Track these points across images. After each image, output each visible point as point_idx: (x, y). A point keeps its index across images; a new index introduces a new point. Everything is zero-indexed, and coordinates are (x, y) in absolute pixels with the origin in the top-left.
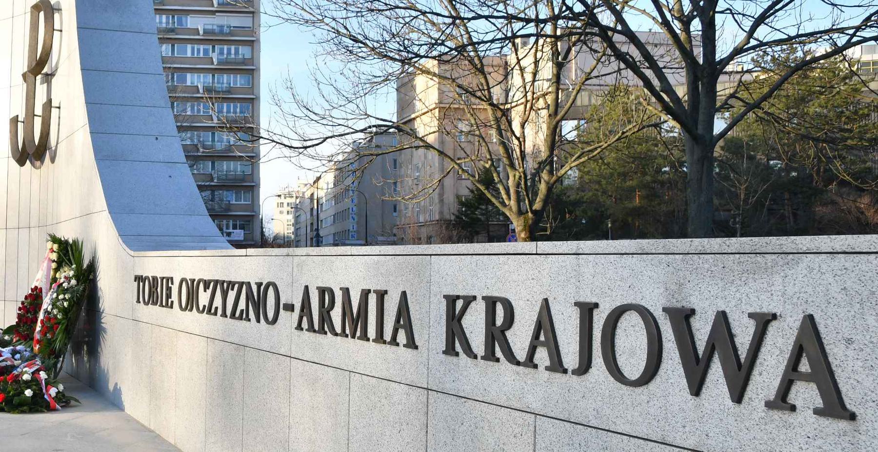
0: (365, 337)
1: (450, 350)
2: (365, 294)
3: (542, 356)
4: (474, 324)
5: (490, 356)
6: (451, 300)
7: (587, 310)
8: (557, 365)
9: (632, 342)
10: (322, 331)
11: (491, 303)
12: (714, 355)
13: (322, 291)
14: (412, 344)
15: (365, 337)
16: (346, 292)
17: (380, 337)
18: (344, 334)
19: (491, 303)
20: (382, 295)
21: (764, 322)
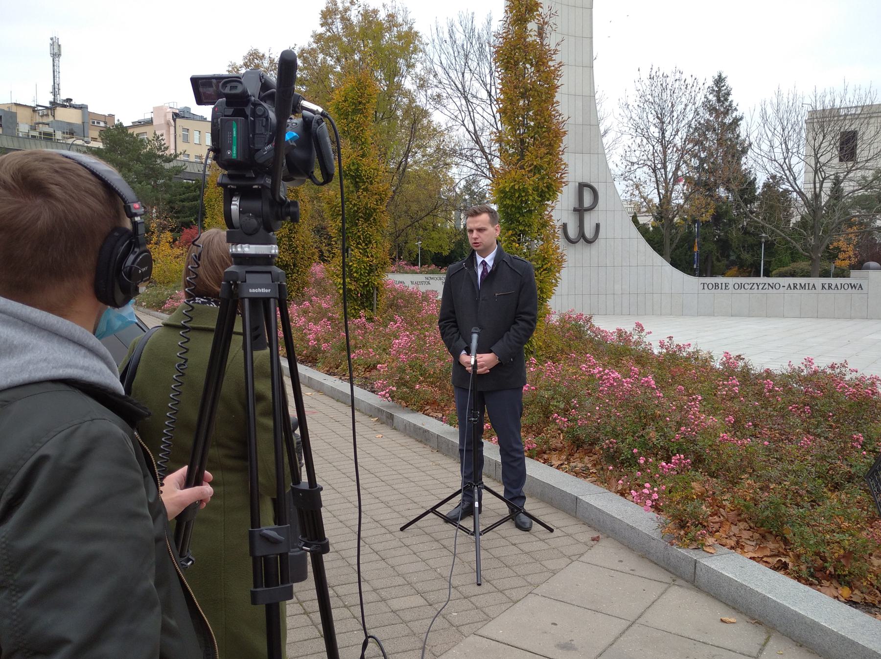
4: (826, 286)
9: (846, 287)
12: (853, 287)
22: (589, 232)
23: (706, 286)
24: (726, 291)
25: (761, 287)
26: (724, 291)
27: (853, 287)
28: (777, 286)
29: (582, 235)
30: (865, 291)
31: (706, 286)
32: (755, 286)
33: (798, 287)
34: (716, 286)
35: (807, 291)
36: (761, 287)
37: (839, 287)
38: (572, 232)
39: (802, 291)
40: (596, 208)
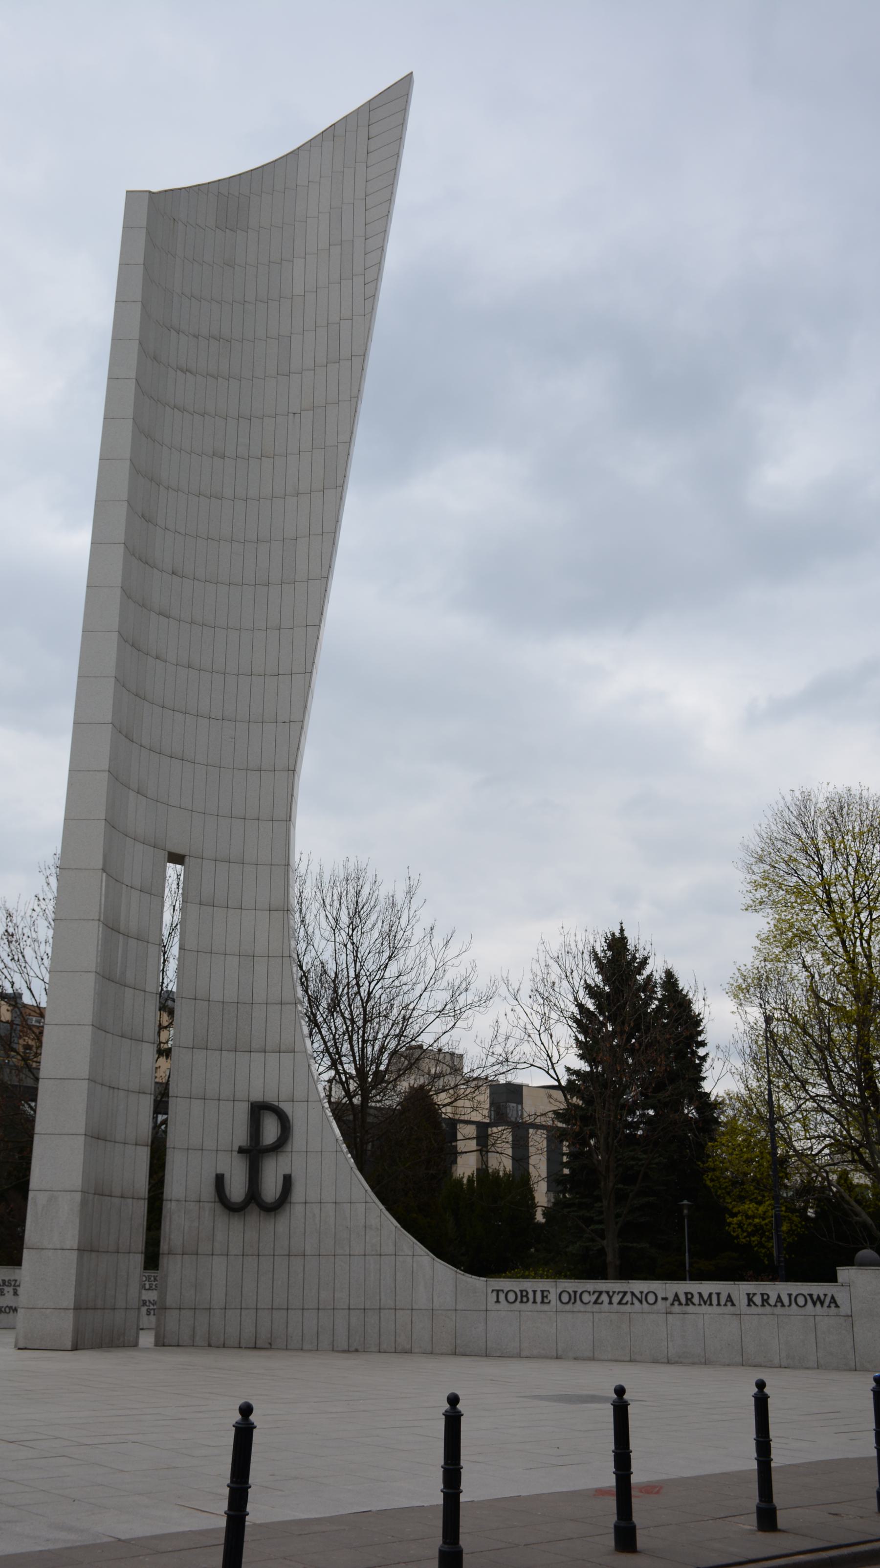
0: (711, 1304)
1: (749, 1305)
2: (710, 1295)
3: (779, 1304)
4: (758, 1300)
5: (763, 1305)
6: (748, 1295)
7: (790, 1295)
8: (783, 1305)
9: (801, 1301)
10: (687, 1304)
11: (762, 1295)
12: (818, 1301)
13: (686, 1294)
14: (733, 1305)
15: (711, 1304)
16: (700, 1294)
17: (719, 1304)
18: (700, 1305)
19: (762, 1295)
20: (718, 1294)
21: (825, 1295)
22: (271, 1189)
23: (502, 1296)
24: (545, 1307)
25: (616, 1299)
26: (538, 1306)
27: (818, 1301)
28: (651, 1298)
29: (253, 1195)
30: (844, 1309)
31: (502, 1296)
32: (605, 1298)
33: (696, 1300)
34: (523, 1297)
35: (715, 1309)
36: (616, 1299)
37: (786, 1301)
38: (237, 1190)
39: (705, 1309)
40: (288, 1148)
